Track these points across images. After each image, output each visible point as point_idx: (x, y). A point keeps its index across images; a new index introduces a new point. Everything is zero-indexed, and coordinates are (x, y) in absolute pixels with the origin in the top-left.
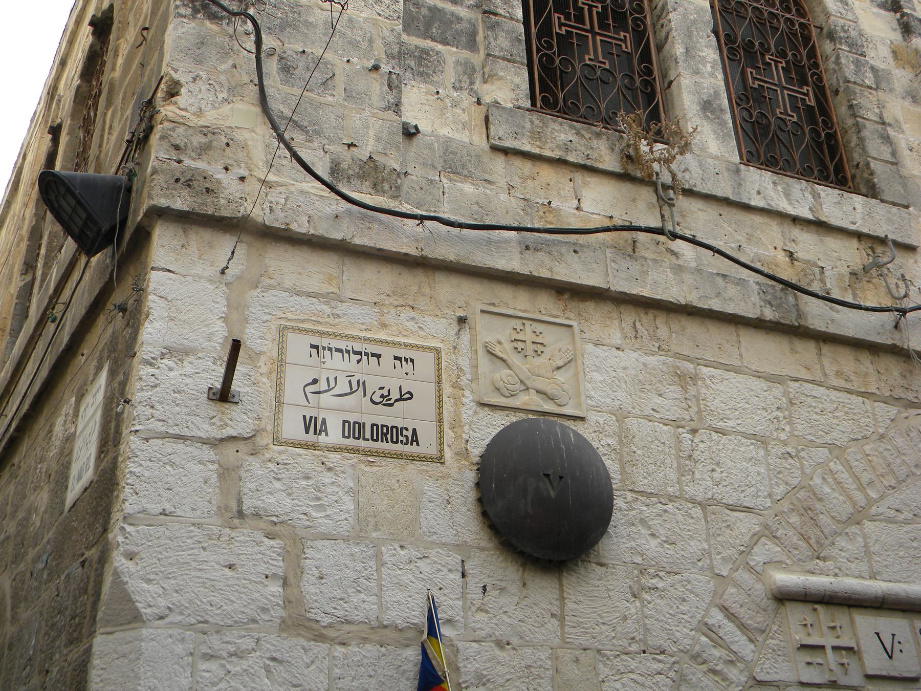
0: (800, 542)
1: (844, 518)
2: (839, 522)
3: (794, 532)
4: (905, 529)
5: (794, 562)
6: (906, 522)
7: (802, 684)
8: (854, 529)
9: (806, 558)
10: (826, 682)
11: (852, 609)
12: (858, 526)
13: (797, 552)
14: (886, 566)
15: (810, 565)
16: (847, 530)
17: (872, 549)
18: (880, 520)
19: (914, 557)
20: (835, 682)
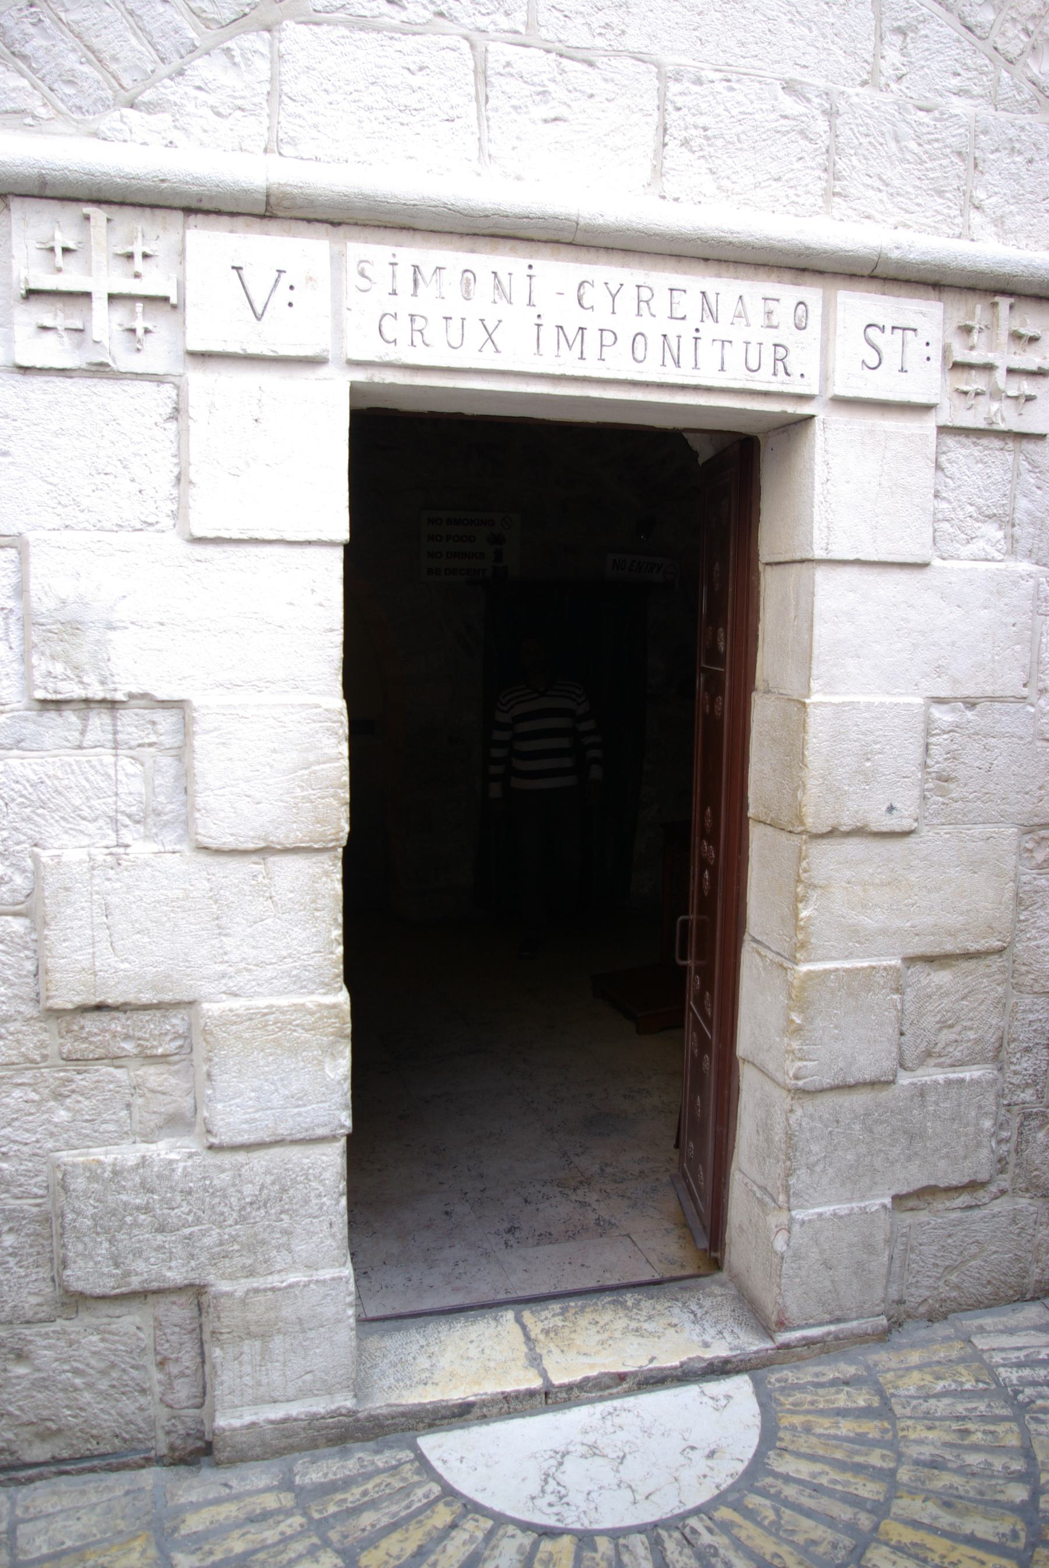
0: (86, 69)
1: (229, 15)
2: (207, 22)
3: (73, 42)
4: (398, 45)
5: (59, 112)
6: (409, 29)
7: (25, 370)
8: (256, 41)
9: (95, 103)
10: (84, 366)
11: (193, 219)
12: (266, 35)
13: (69, 90)
14: (315, 126)
15: (109, 121)
16: (229, 44)
17: (286, 89)
18: (335, 23)
19: (405, 109)
20: (102, 364)
